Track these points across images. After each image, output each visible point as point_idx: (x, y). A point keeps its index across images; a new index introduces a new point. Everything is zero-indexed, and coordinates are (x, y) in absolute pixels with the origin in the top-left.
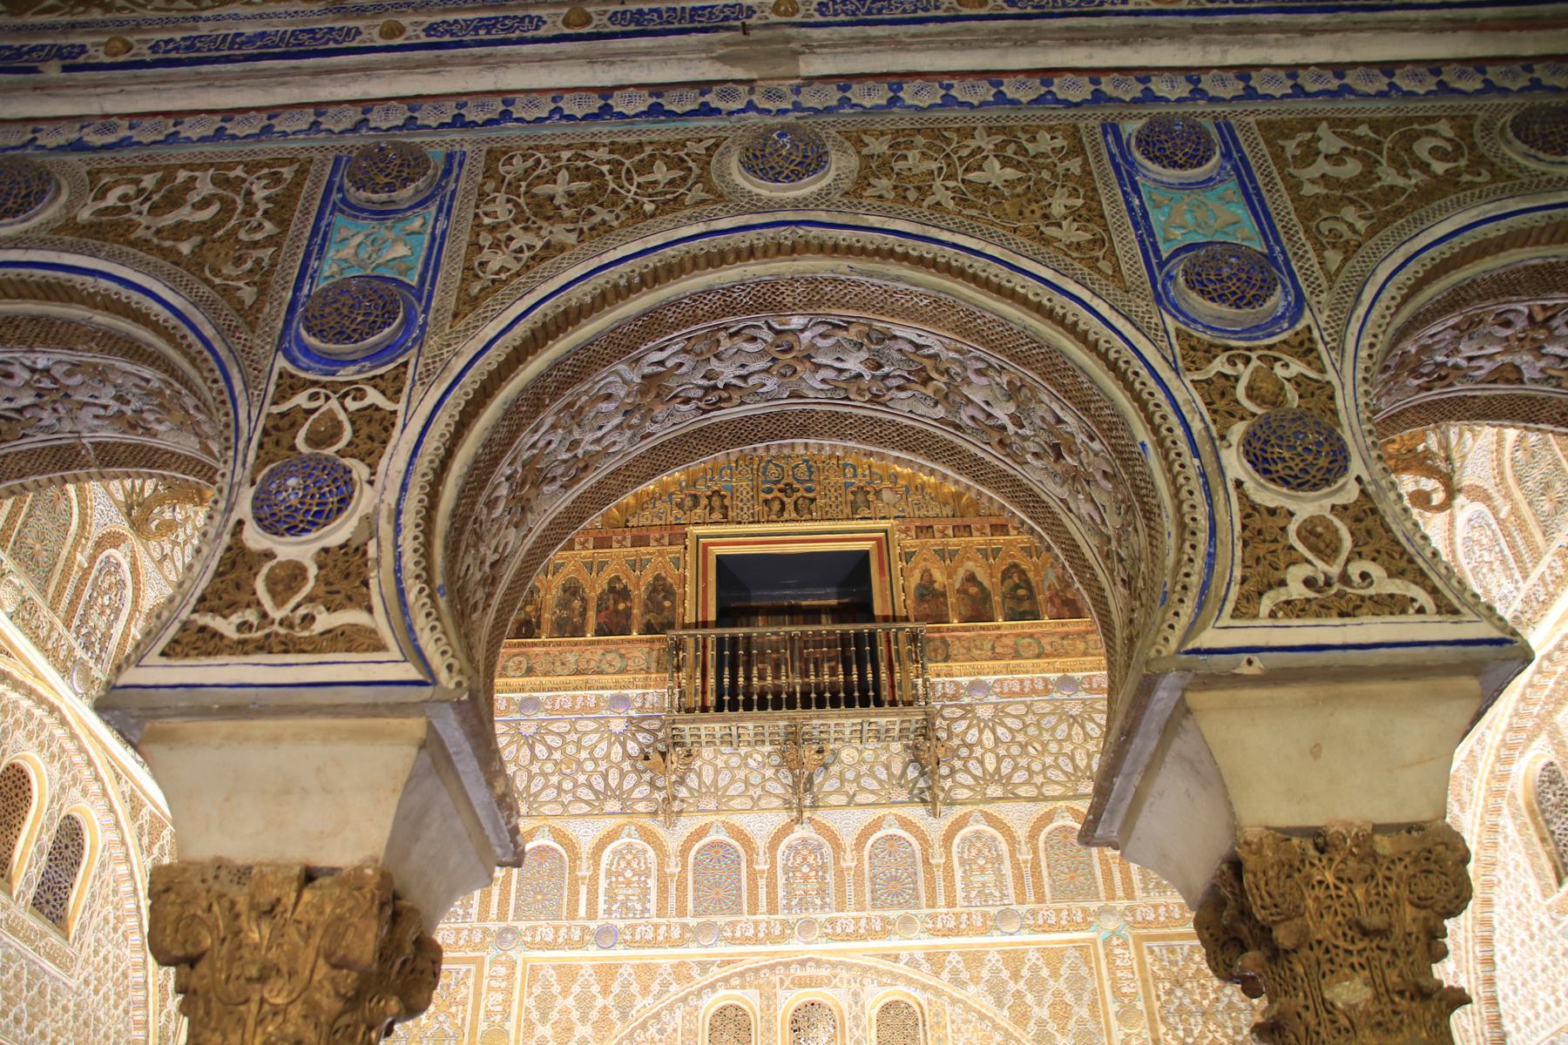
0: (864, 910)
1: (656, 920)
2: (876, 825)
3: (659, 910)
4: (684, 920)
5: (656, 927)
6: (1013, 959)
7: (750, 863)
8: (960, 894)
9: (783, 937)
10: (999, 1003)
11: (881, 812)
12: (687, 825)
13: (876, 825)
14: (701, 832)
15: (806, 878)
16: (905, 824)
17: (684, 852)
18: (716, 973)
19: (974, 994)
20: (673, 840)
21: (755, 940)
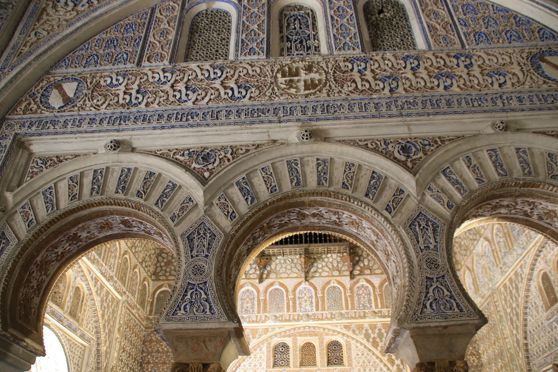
0: (325, 310)
1: (257, 314)
2: (329, 283)
3: (258, 311)
4: (266, 314)
5: (257, 316)
6: (373, 327)
7: (287, 296)
8: (356, 305)
9: (298, 320)
10: (368, 341)
11: (330, 278)
12: (266, 282)
13: (329, 283)
14: (272, 284)
15: (306, 301)
16: (339, 283)
17: (265, 292)
18: (277, 330)
19: (361, 338)
20: (262, 287)
21: (289, 321)
